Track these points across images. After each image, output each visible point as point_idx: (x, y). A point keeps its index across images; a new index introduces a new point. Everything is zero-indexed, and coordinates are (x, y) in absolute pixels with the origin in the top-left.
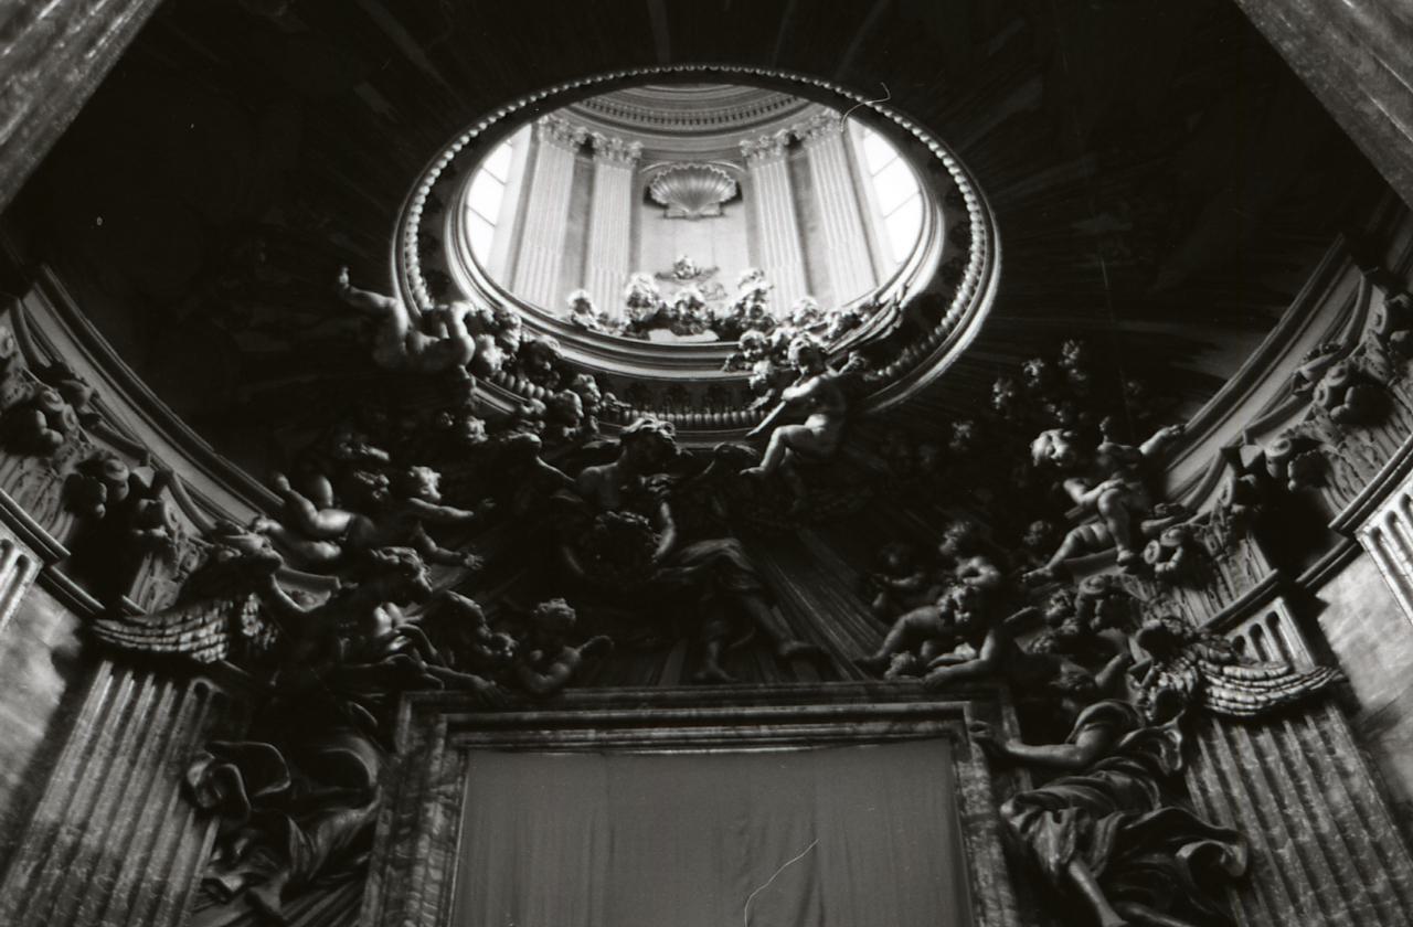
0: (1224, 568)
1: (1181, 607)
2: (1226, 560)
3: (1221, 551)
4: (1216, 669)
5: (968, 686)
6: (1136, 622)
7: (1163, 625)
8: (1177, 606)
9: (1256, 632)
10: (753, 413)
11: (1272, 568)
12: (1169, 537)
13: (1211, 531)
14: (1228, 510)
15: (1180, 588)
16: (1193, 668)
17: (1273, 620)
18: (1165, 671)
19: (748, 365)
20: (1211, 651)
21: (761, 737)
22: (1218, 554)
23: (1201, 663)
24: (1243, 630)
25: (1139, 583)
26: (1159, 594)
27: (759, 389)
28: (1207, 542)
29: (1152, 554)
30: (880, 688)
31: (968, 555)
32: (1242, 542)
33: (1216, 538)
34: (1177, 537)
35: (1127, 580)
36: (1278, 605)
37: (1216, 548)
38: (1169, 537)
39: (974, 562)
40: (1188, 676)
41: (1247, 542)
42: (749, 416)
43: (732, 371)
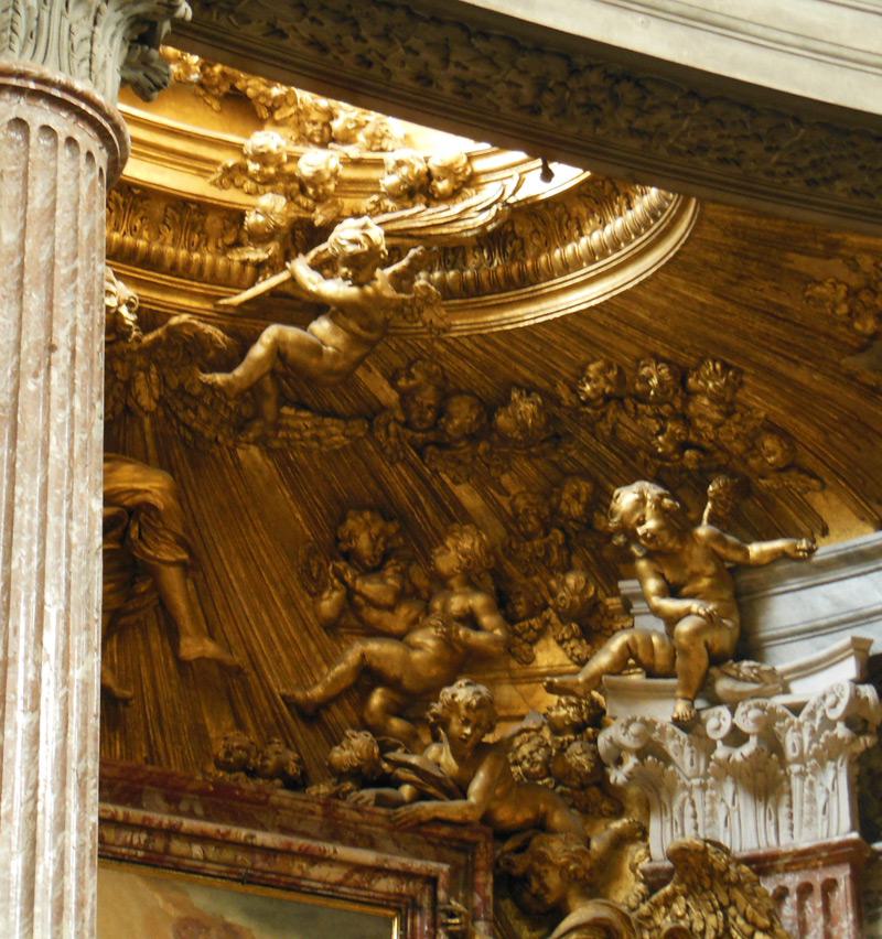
0: (796, 783)
1: (727, 807)
2: (802, 775)
3: (801, 759)
4: (748, 929)
5: (445, 831)
6: (664, 798)
7: (706, 849)
8: (723, 805)
9: (805, 890)
10: (236, 266)
11: (853, 829)
12: (747, 718)
13: (800, 728)
14: (828, 724)
15: (735, 782)
16: (720, 913)
17: (830, 886)
18: (686, 897)
19: (249, 185)
20: (749, 908)
21: (191, 858)
22: (796, 761)
23: (732, 911)
24: (792, 881)
25: (687, 750)
26: (706, 776)
27: (260, 237)
28: (790, 740)
29: (718, 728)
30: (341, 811)
31: (471, 583)
32: (830, 765)
33: (801, 740)
34: (757, 721)
35: (673, 735)
36: (842, 874)
37: (796, 754)
38: (747, 718)
39: (478, 601)
40: (712, 920)
41: (836, 768)
42: (228, 270)
43: (222, 187)
